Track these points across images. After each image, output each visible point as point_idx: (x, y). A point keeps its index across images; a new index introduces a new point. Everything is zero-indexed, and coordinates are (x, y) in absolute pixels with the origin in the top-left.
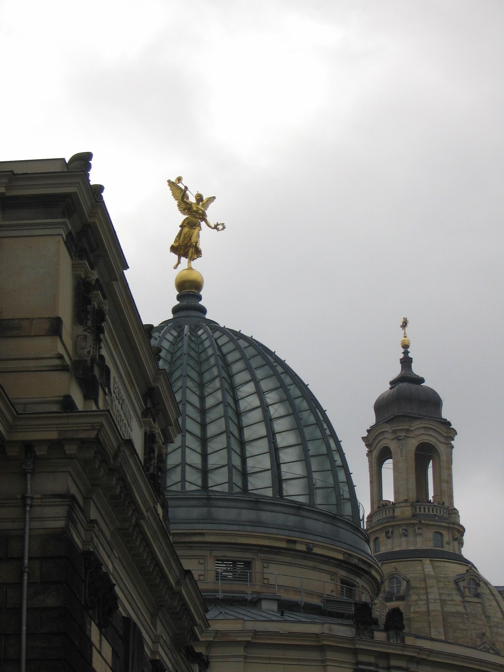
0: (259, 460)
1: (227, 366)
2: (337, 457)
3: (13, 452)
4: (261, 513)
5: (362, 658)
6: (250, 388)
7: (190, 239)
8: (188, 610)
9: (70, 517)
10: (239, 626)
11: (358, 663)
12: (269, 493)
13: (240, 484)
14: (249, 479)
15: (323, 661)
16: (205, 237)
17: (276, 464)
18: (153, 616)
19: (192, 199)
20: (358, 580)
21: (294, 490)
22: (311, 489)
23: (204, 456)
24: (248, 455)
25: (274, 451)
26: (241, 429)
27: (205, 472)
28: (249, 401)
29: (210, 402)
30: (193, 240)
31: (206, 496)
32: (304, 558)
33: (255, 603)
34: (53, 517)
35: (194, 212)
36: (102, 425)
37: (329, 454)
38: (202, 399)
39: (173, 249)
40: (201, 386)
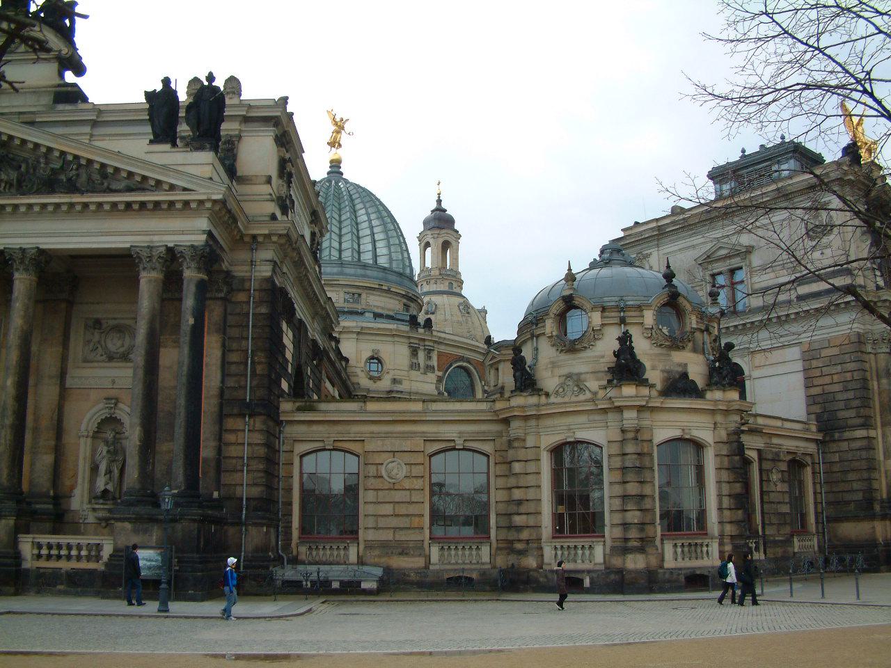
0: (366, 246)
2: (404, 246)
3: (247, 239)
5: (412, 341)
6: (363, 211)
8: (329, 316)
9: (274, 271)
10: (354, 324)
12: (371, 262)
16: (344, 138)
17: (375, 248)
18: (313, 318)
19: (338, 120)
22: (391, 260)
23: (340, 244)
25: (374, 242)
27: (340, 251)
28: (362, 217)
31: (341, 263)
33: (362, 314)
34: (265, 271)
35: (339, 126)
36: (290, 228)
37: (400, 244)
38: (340, 216)
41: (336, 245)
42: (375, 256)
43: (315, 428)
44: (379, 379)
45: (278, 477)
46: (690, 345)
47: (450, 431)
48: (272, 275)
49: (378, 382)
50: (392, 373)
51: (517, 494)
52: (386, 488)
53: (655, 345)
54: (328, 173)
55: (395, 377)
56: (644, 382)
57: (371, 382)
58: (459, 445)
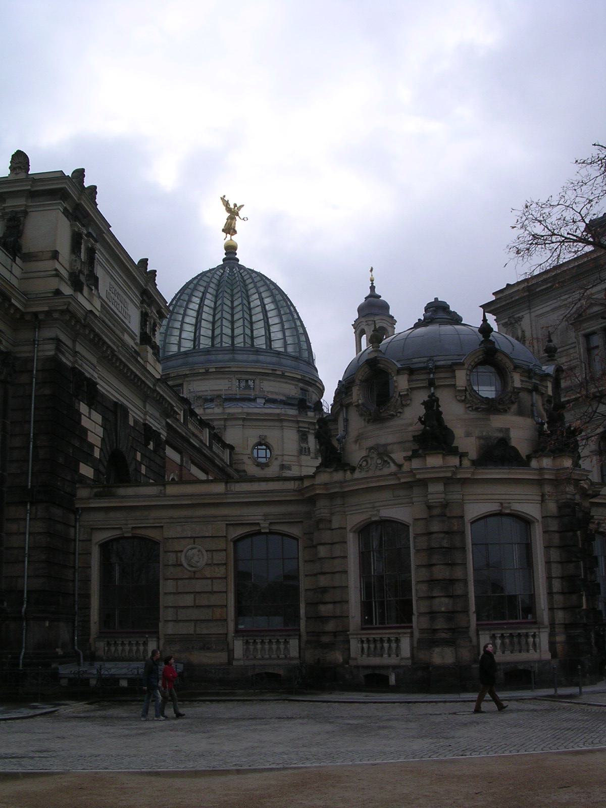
0: (259, 331)
1: (246, 285)
3: (28, 318)
4: (259, 356)
5: (301, 425)
7: (231, 225)
8: (164, 399)
9: (58, 349)
10: (240, 410)
11: (299, 427)
13: (250, 343)
14: (255, 340)
15: (282, 426)
16: (239, 224)
18: (144, 402)
20: (310, 388)
21: (277, 345)
22: (285, 345)
23: (233, 330)
24: (254, 329)
26: (251, 316)
27: (233, 337)
29: (236, 303)
30: (233, 225)
31: (233, 349)
32: (281, 378)
33: (254, 400)
34: (49, 350)
35: (233, 213)
36: (70, 303)
37: (296, 328)
38: (232, 302)
39: (223, 230)
40: (232, 296)
41: (229, 332)
42: (269, 340)
43: (112, 514)
44: (266, 465)
45: (74, 567)
46: (514, 407)
47: (255, 514)
48: (56, 354)
49: (267, 469)
50: (280, 458)
51: (323, 581)
52: (187, 577)
53: (470, 409)
54: (224, 260)
55: (284, 463)
56: (454, 451)
57: (259, 468)
58: (264, 528)
